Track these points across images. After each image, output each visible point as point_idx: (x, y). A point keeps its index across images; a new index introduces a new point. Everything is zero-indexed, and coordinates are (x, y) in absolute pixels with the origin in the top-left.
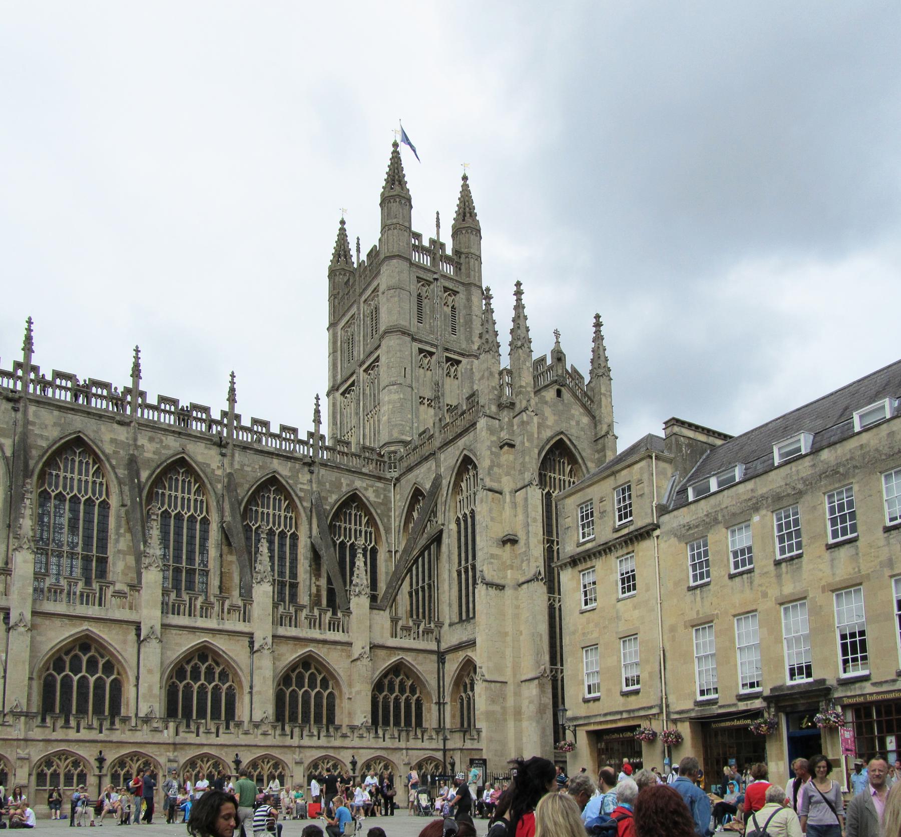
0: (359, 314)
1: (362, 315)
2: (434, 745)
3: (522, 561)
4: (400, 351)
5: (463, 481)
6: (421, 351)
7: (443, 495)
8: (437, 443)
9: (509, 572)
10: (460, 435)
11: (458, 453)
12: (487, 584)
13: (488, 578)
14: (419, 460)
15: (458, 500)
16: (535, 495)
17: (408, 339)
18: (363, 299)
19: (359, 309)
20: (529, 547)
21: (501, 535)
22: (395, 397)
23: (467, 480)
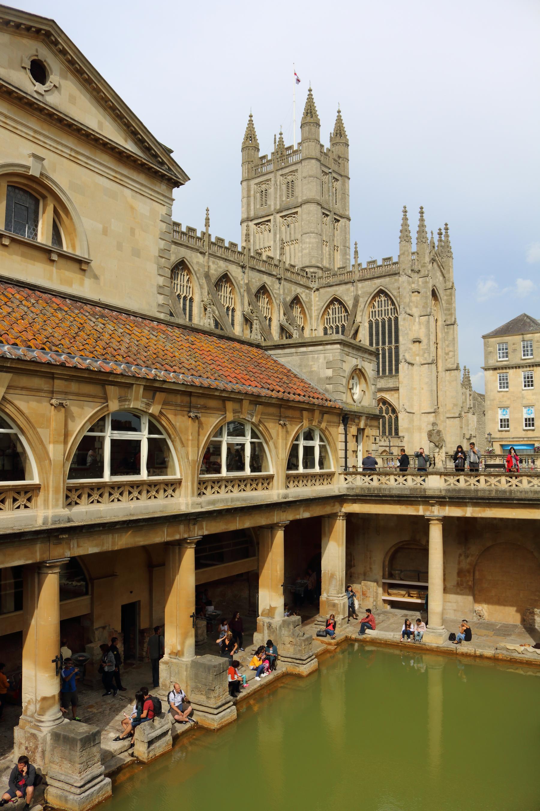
0: (276, 181)
1: (278, 183)
2: (385, 445)
3: (424, 353)
4: (317, 214)
5: (375, 301)
6: (324, 214)
7: (360, 306)
8: (357, 277)
9: (417, 358)
10: (378, 277)
11: (374, 287)
12: (409, 363)
13: (408, 360)
14: (338, 283)
15: (371, 311)
16: (432, 319)
17: (320, 207)
18: (280, 172)
19: (275, 177)
20: (430, 346)
21: (412, 338)
22: (314, 240)
23: (378, 301)
